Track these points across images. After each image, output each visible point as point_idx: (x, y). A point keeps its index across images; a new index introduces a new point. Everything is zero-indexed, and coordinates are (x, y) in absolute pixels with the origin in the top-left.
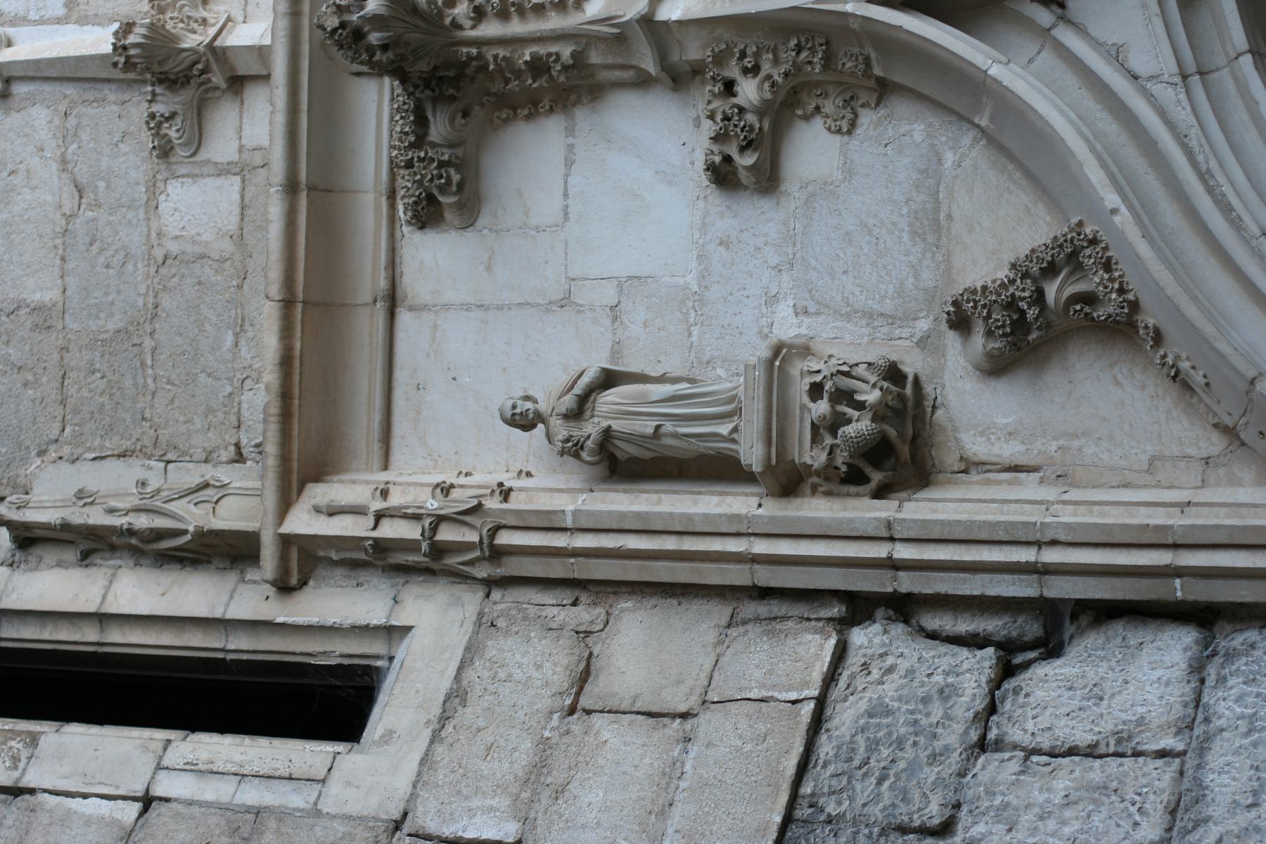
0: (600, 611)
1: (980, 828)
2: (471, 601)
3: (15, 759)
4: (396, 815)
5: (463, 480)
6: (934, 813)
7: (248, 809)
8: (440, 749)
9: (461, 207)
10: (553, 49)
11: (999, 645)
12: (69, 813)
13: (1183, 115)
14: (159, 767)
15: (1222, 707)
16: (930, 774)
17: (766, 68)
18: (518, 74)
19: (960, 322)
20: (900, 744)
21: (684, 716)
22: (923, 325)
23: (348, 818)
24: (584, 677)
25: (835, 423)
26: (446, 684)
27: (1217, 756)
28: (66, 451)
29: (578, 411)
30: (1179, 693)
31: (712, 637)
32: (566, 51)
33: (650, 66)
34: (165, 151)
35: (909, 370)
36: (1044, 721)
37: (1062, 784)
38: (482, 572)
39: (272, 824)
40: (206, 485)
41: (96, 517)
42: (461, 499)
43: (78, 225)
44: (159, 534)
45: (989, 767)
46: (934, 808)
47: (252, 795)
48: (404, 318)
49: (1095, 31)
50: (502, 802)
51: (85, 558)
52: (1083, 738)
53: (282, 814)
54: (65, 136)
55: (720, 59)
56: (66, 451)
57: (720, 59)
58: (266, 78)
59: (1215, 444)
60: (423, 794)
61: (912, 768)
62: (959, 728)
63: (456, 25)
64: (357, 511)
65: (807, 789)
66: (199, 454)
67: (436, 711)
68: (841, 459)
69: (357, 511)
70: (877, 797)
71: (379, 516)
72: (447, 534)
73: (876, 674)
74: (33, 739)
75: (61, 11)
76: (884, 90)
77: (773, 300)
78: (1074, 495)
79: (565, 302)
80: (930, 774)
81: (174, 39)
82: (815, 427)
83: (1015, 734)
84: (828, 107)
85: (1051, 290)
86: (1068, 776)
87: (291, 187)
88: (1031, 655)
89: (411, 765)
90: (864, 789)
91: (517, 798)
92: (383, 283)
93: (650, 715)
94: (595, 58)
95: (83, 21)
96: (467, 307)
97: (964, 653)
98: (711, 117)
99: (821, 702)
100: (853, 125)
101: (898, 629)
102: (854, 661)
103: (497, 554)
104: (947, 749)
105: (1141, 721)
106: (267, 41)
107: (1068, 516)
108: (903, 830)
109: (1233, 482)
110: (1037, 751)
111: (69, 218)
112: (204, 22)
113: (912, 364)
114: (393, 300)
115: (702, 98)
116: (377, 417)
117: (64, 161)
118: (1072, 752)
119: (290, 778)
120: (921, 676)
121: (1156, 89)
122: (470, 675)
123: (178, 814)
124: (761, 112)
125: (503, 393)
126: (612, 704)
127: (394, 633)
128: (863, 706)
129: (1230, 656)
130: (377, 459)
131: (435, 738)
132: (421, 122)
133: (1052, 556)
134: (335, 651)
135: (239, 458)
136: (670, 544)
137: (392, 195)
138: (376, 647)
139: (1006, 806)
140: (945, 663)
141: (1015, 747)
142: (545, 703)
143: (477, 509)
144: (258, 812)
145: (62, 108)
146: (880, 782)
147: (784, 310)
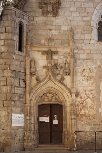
6: (17, 77)
27: (20, 88)
45: (19, 79)
72: (28, 55)
80: (18, 77)
86: (19, 82)
95: (52, 35)
113: (36, 75)
131: (19, 55)
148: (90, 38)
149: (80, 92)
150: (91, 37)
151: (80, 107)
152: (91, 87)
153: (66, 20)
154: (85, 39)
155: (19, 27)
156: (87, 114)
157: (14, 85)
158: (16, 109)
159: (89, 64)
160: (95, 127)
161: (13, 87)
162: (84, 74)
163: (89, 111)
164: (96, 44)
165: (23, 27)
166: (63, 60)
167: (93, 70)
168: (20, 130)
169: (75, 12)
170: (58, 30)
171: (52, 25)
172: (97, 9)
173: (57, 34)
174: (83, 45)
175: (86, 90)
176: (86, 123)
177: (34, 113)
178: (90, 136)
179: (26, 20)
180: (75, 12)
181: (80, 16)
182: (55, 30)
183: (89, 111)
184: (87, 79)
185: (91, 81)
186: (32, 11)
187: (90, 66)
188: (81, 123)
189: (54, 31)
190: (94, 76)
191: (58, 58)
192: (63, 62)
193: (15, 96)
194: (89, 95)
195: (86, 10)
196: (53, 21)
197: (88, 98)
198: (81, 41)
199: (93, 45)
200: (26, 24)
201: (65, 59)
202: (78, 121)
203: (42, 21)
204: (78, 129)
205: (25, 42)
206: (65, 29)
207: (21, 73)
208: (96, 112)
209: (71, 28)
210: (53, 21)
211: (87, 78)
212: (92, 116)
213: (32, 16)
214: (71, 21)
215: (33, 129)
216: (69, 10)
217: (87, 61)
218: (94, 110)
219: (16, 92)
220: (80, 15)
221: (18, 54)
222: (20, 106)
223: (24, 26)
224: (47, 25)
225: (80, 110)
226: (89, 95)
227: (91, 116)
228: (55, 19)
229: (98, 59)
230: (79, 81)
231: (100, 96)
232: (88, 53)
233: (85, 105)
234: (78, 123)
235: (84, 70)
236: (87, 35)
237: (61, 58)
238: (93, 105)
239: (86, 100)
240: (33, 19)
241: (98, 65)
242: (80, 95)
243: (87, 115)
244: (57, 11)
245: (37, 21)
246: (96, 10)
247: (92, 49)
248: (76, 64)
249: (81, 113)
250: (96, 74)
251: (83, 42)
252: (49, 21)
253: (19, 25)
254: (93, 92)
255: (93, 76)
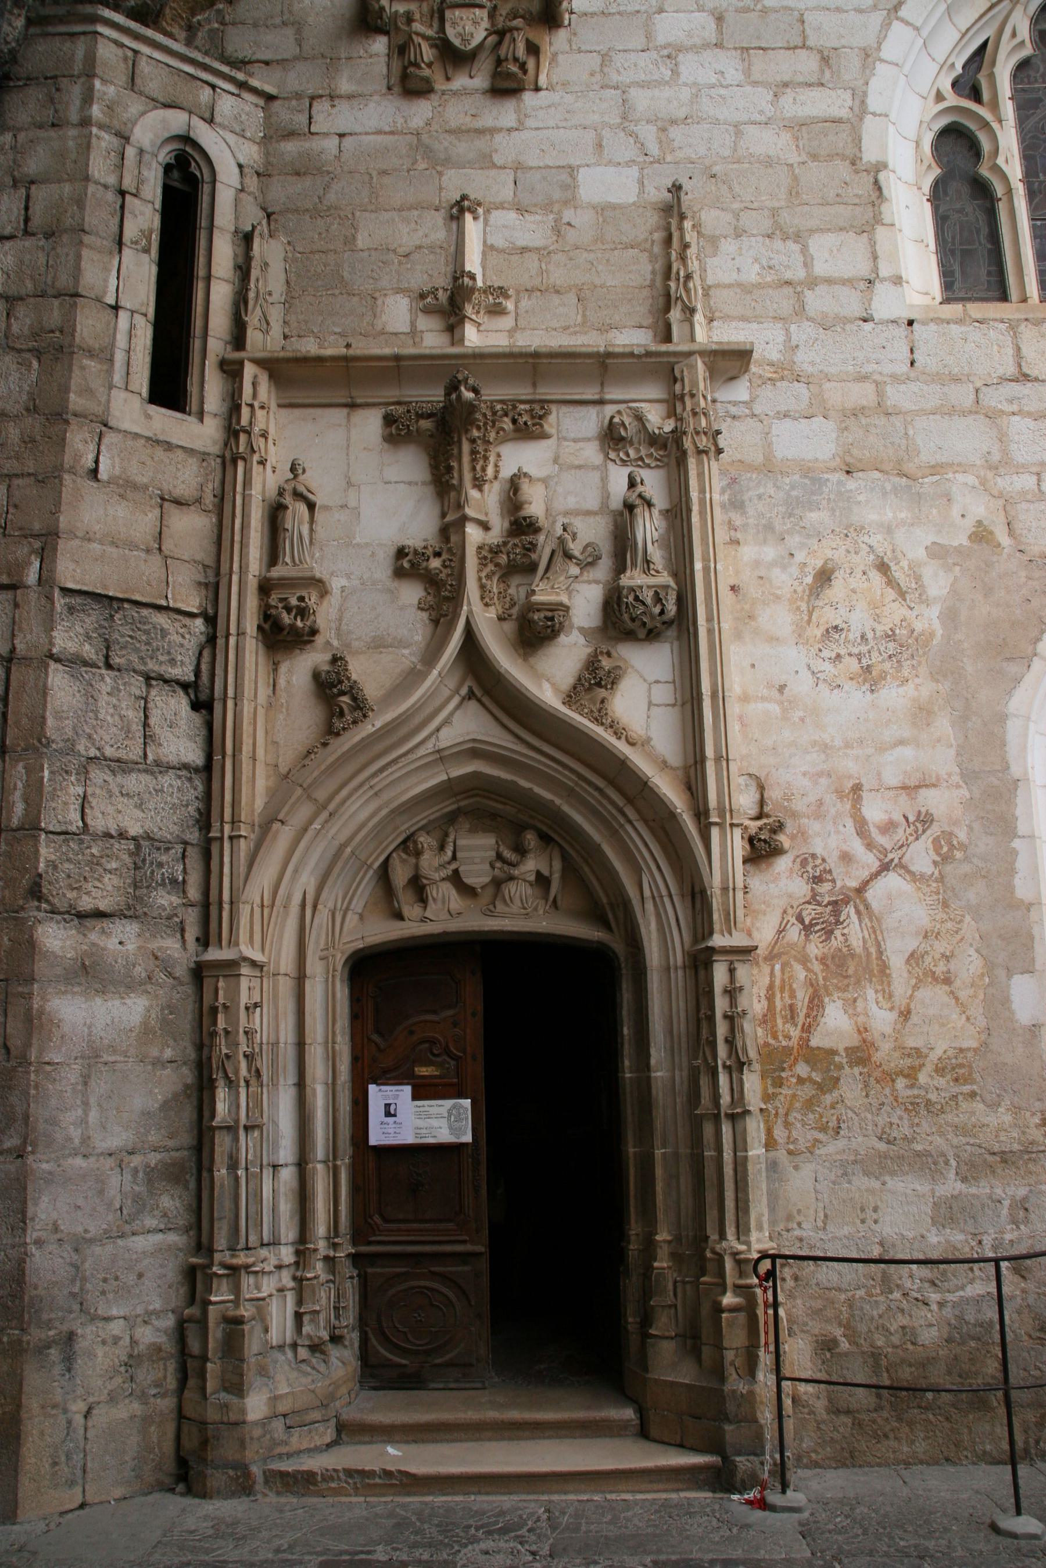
0: (211, 507)
1: (108, 680)
2: (215, 449)
3: (136, 243)
4: (110, 424)
5: (270, 441)
6: (116, 660)
7: (112, 356)
8: (143, 441)
9: (391, 435)
10: (456, 475)
11: (196, 682)
12: (109, 271)
13: (422, 752)
14: (133, 312)
15: (167, 778)
16: (134, 658)
17: (446, 571)
18: (447, 460)
19: (335, 660)
20: (148, 643)
21: (160, 549)
22: (335, 643)
23: (108, 401)
24: (178, 503)
25: (288, 609)
26: (174, 441)
27: (145, 778)
28: (290, 255)
29: (298, 495)
30: (173, 759)
31: (198, 558)
32: (455, 482)
33: (448, 518)
34: (422, 296)
35: (316, 637)
36: (160, 704)
37: (131, 714)
38: (228, 455)
39: (105, 367)
40: (268, 324)
41: (255, 273)
42: (259, 443)
43: (392, 256)
44: (246, 303)
46: (118, 660)
47: (119, 357)
48: (344, 411)
49: (458, 712)
50: (117, 471)
51: (238, 267)
52: (152, 721)
53: (110, 372)
54: (431, 248)
55: (450, 550)
56: (290, 255)
57: (450, 550)
58: (453, 344)
59: (283, 770)
60: (121, 436)
61: (137, 650)
62: (156, 668)
63: (467, 431)
64: (255, 396)
65: (126, 605)
66: (288, 318)
67: (161, 438)
68: (273, 611)
69: (255, 396)
70: (122, 636)
71: (251, 406)
72: (243, 438)
73: (181, 631)
74: (146, 251)
75: (489, 242)
76: (436, 622)
77: (348, 576)
78: (261, 712)
79: (350, 484)
80: (134, 658)
81: (469, 300)
82: (286, 599)
83: (154, 692)
84: (429, 598)
85: (345, 699)
86: (134, 716)
87: (397, 358)
88: (192, 696)
89: (135, 429)
90: (126, 630)
91: (119, 478)
92: (359, 401)
93: (160, 533)
94: (453, 494)
95: (484, 253)
96: (348, 439)
97: (191, 668)
98: (425, 548)
99: (167, 608)
100: (422, 609)
101: (203, 639)
102: (187, 621)
103: (234, 461)
104: (145, 664)
105: (160, 745)
106: (467, 343)
107: (247, 708)
108: (108, 648)
109: (268, 777)
110: (146, 703)
111: (394, 251)
112: (478, 312)
113: (319, 640)
114: (352, 406)
115: (434, 542)
116: (300, 401)
117: (420, 247)
118: (146, 717)
119: (128, 374)
120: (180, 650)
121: (433, 740)
122: (179, 452)
123: (108, 324)
124: (426, 569)
125: (305, 460)
126: (165, 517)
127: (201, 415)
128: (166, 626)
129: (190, 779)
130: (281, 402)
131: (148, 439)
132: (429, 416)
133: (230, 704)
134: (193, 388)
135: (285, 337)
136: (237, 538)
137: (399, 403)
138: (195, 407)
139: (119, 691)
140: (187, 660)
141: (148, 692)
142: (165, 487)
143: (253, 451)
144: (111, 360)
145: (445, 245)
146: (131, 637)
147: (344, 582)
148: (863, 268)
149: (799, 805)
150: (875, 258)
151: (801, 974)
152: (907, 752)
153: (624, 118)
154: (813, 282)
155: (167, 189)
156: (886, 1047)
157: (80, 748)
158: (99, 1001)
159: (873, 517)
160: (981, 1189)
161: (74, 763)
162: (829, 616)
163: (906, 1014)
164: (924, 323)
165: (207, 188)
166: (604, 480)
167: (918, 578)
168: (142, 1243)
169: (706, 46)
170: (547, 207)
171: (486, 162)
172: (907, 23)
173: (539, 243)
174: (802, 332)
175: (857, 788)
176: (882, 1146)
177: (301, 1045)
178: (934, 1297)
179: (237, 129)
180: (706, 46)
181: (755, 83)
182: (521, 210)
183: (906, 1014)
184: (868, 669)
185: (909, 689)
186: (296, 58)
187: (889, 530)
188: (820, 1151)
189: (512, 215)
190: (939, 632)
191: (556, 460)
192: (606, 496)
193: (95, 863)
194: (900, 835)
195: (808, 31)
196: (492, 131)
197: (885, 867)
198: (783, 302)
199: (902, 331)
200: (240, 166)
201: (625, 471)
202: (787, 1125)
203: (392, 133)
204: (789, 1218)
205: (219, 322)
206: (613, 199)
207: (161, 620)
208: (981, 1022)
209: (676, 188)
210: (500, 130)
211: (859, 657)
212: (940, 1070)
213: (298, 96)
214: (673, 122)
215: (288, 1233)
216: (649, 37)
217: (851, 484)
218: (963, 995)
219: (98, 822)
220: (756, 76)
221: (136, 436)
222: (139, 971)
223: (214, 181)
224: (439, 163)
225: (802, 997)
226: (900, 835)
227: (929, 1068)
228: (518, 111)
229: (962, 468)
230: (782, 688)
231: (1016, 844)
232: (857, 413)
233: (856, 943)
234: (790, 1153)
235: (824, 577)
236: (830, 239)
237: (579, 467)
238: (941, 947)
239: (866, 883)
240: (303, 119)
241: (969, 524)
242: (802, 834)
243: (884, 1053)
244: (534, 50)
245: (341, 136)
246: (896, 25)
247: (888, 369)
248: (744, 513)
249: (814, 1043)
250: (950, 617)
251: (800, 311)
252: (457, 132)
253: (168, 169)
254: (934, 800)
255: (924, 640)
